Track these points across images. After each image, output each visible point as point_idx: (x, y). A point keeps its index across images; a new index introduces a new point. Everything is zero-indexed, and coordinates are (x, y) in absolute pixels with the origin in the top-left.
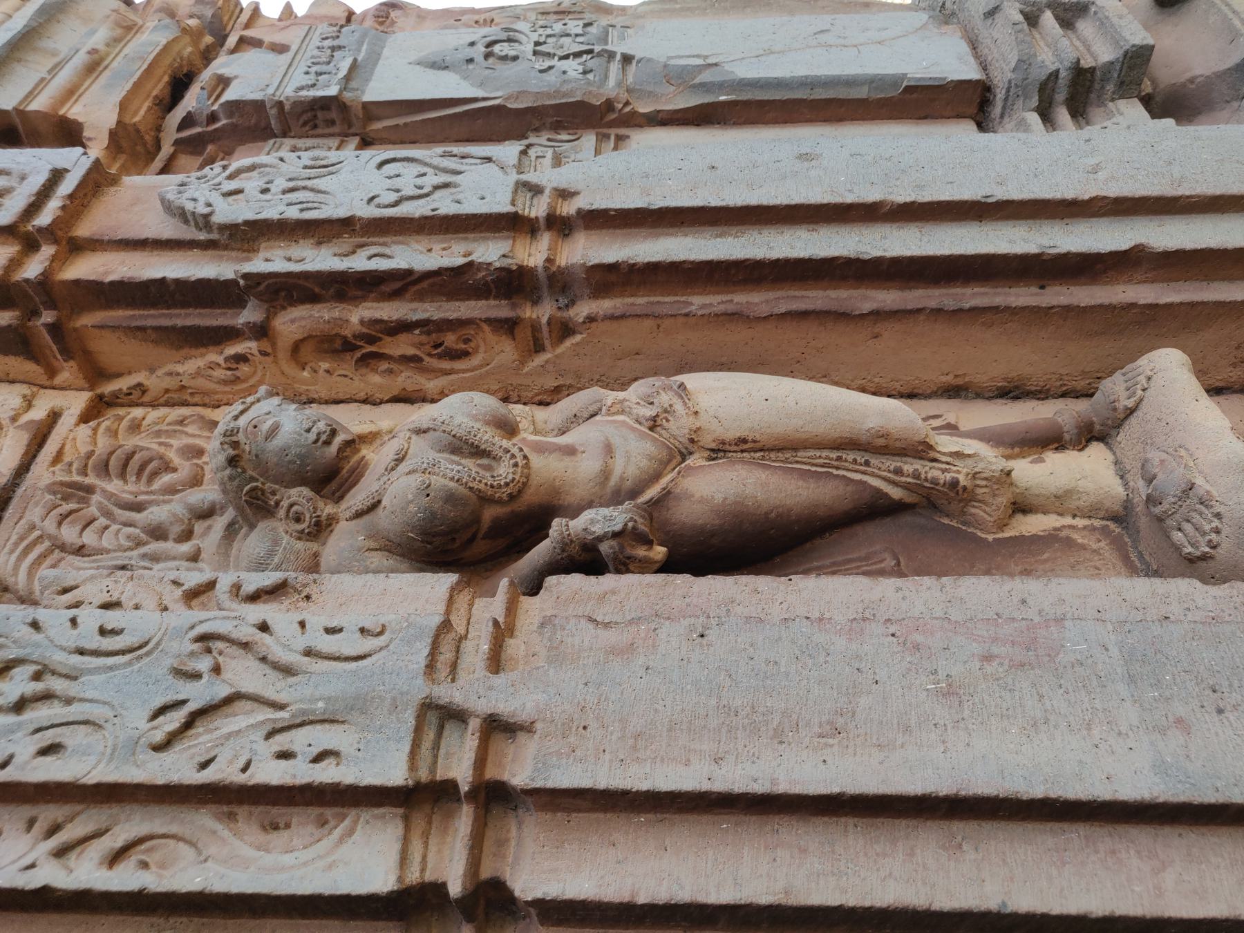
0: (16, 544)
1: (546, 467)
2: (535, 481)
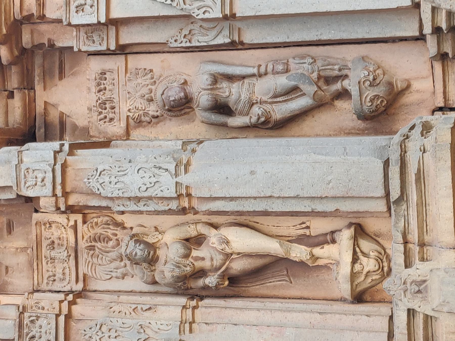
0: (85, 265)
1: (199, 264)
2: (196, 267)
